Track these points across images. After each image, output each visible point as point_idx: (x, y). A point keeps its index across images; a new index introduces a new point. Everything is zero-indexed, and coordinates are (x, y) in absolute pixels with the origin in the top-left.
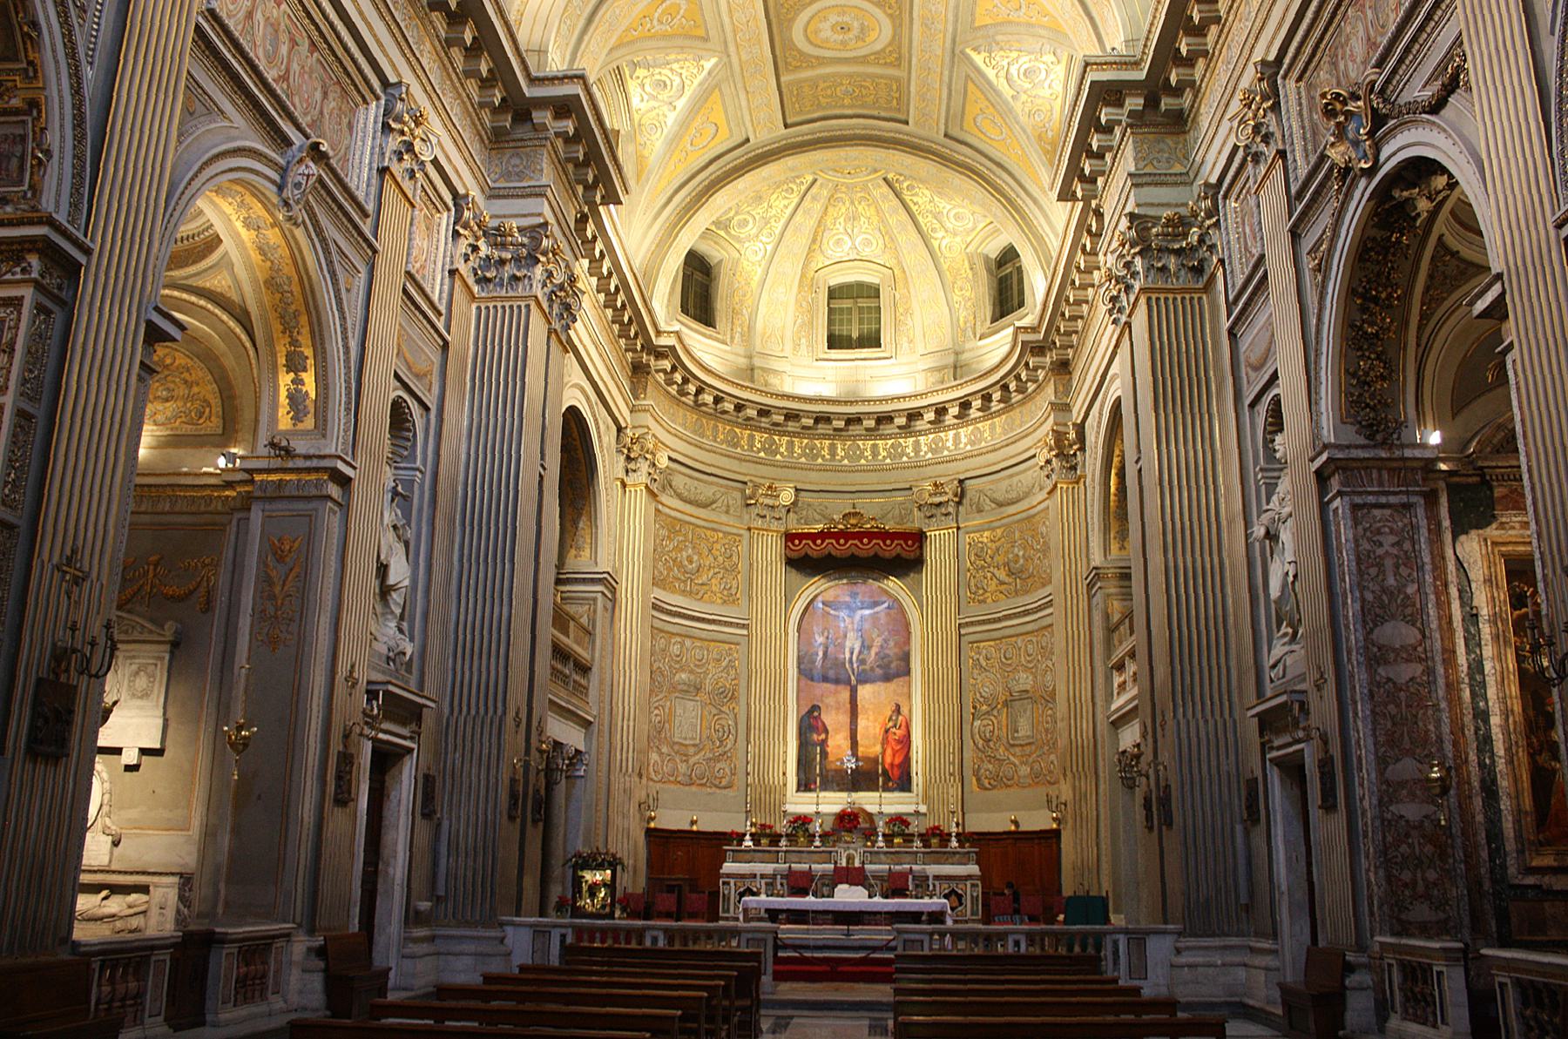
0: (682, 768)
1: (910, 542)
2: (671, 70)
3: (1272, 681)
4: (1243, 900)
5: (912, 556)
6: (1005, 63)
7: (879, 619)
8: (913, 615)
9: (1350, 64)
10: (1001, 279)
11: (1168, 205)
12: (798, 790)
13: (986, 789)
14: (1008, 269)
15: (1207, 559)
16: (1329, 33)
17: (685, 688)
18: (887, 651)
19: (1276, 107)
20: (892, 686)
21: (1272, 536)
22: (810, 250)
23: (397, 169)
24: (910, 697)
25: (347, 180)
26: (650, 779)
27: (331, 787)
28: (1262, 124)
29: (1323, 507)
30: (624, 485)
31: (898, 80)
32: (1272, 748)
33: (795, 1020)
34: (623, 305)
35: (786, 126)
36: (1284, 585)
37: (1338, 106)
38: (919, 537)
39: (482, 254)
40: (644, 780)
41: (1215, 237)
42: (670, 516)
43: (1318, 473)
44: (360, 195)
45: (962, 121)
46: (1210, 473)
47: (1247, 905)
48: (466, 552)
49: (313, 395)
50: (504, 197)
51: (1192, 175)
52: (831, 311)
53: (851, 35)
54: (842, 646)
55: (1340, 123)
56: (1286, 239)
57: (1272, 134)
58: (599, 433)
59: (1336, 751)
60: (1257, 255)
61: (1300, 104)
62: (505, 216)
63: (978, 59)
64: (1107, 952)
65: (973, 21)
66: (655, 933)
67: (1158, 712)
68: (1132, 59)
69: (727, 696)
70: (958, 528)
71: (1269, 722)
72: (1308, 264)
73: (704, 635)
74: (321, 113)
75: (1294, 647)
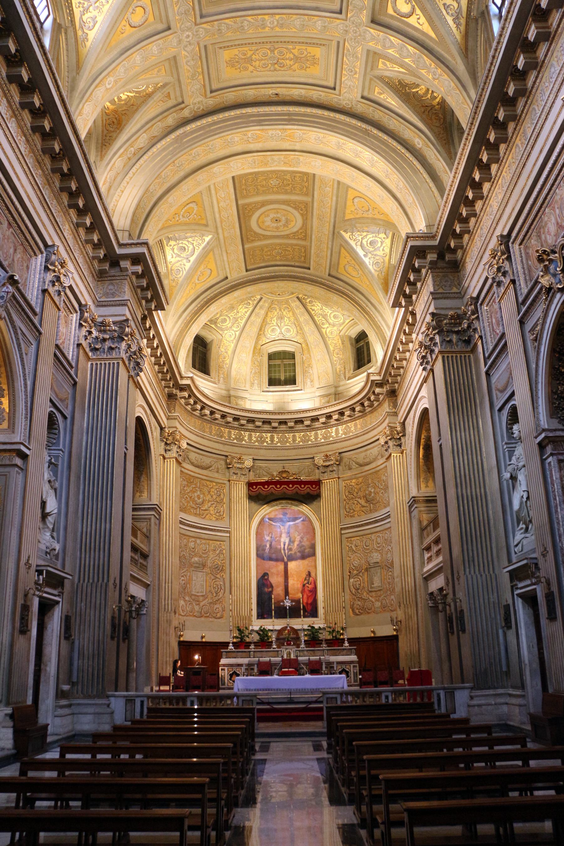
0: (197, 608)
2: (188, 241)
3: (516, 553)
4: (504, 669)
5: (315, 493)
6: (360, 238)
7: (298, 527)
8: (317, 525)
9: (548, 237)
11: (451, 309)
12: (258, 618)
13: (357, 615)
14: (361, 343)
15: (478, 490)
16: (536, 221)
17: (197, 565)
19: (509, 258)
20: (306, 562)
21: (513, 478)
22: (259, 335)
23: (51, 290)
25: (26, 295)
26: (180, 615)
27: (18, 625)
28: (501, 267)
29: (543, 461)
30: (164, 458)
31: (305, 247)
32: (517, 588)
33: (272, 744)
34: (164, 363)
35: (247, 271)
36: (521, 503)
37: (545, 257)
38: (318, 483)
39: (93, 336)
40: (177, 615)
41: (476, 324)
43: (540, 444)
44: (33, 303)
45: (338, 268)
46: (478, 446)
47: (506, 672)
48: (86, 494)
49: (7, 410)
50: (105, 306)
51: (463, 293)
52: (270, 366)
53: (281, 224)
54: (279, 542)
55: (545, 266)
56: (517, 325)
57: (507, 272)
58: (151, 430)
59: (555, 588)
60: (500, 334)
61: (521, 257)
62: (105, 316)
63: (347, 236)
64: (435, 700)
65: (344, 216)
66: (192, 699)
67: (455, 572)
68: (431, 235)
69: (218, 569)
71: (516, 575)
72: (530, 337)
74: (13, 260)
75: (527, 535)
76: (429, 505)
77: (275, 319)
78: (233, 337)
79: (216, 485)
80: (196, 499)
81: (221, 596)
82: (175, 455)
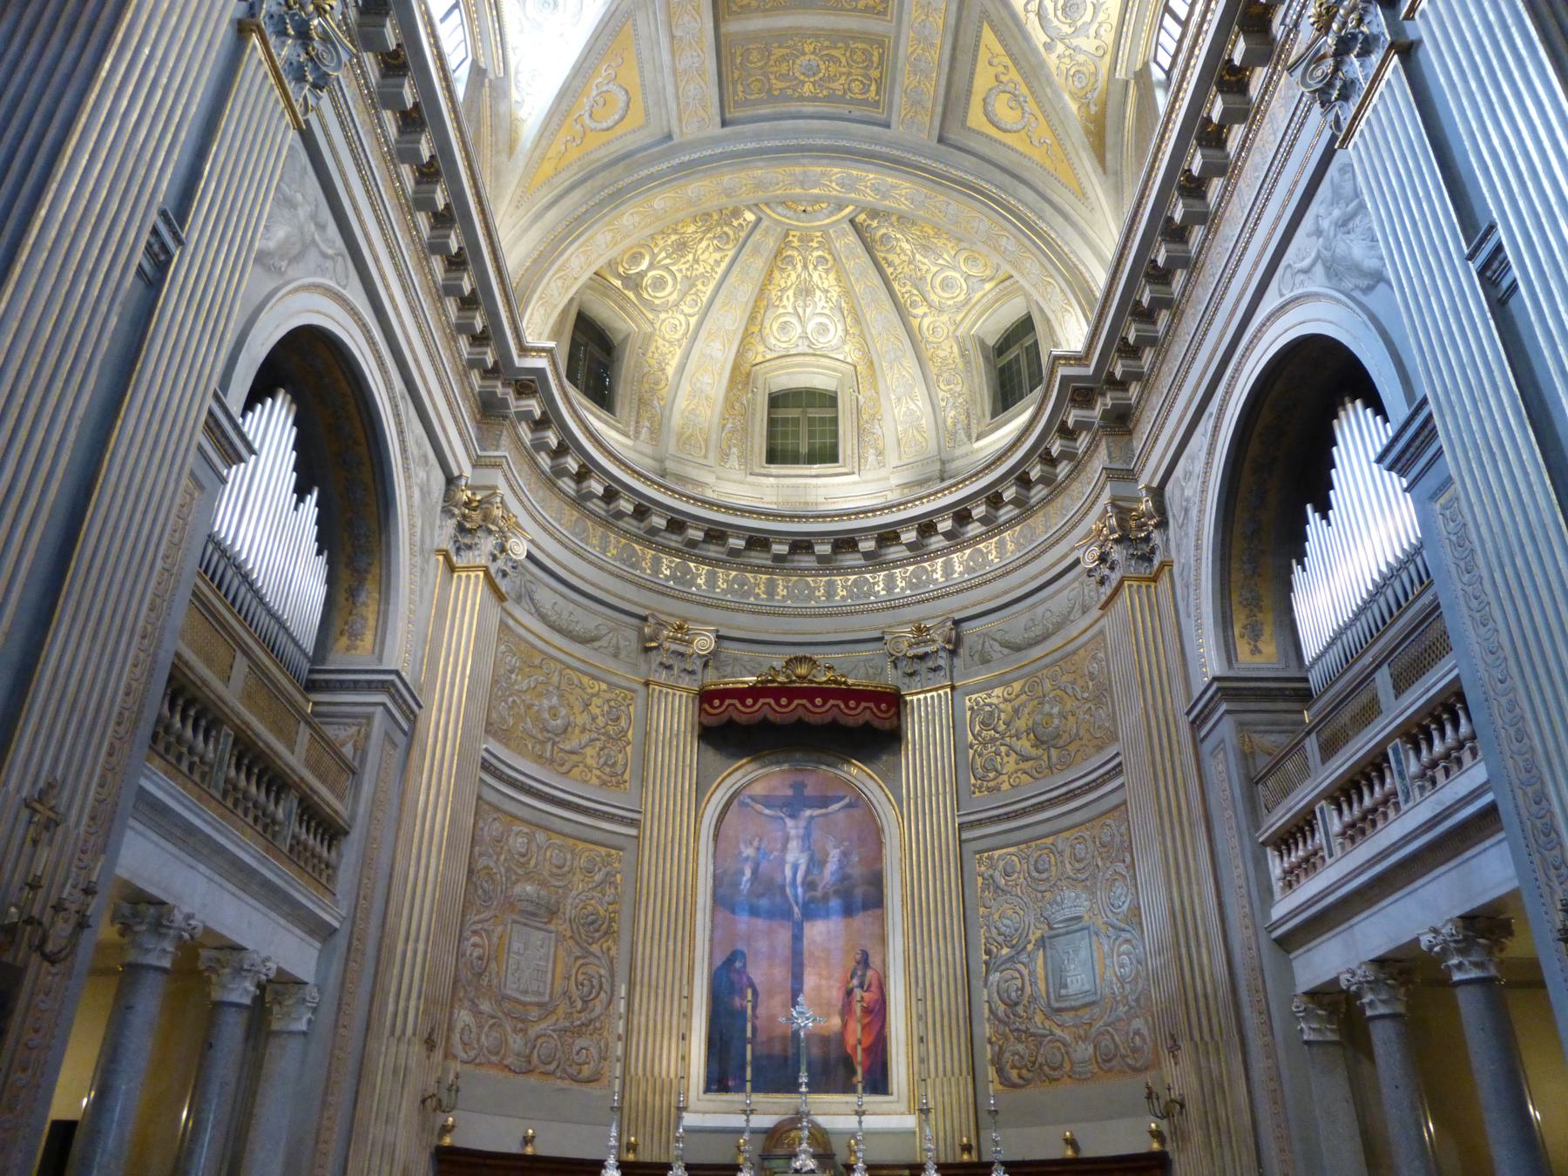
0: (516, 1042)
1: (883, 706)
5: (887, 725)
8: (888, 815)
10: (1002, 371)
12: (707, 1090)
13: (1014, 1086)
18: (849, 870)
22: (747, 334)
24: (883, 940)
30: (452, 568)
35: (724, 123)
38: (893, 701)
40: (438, 1055)
42: (527, 642)
52: (772, 422)
54: (782, 862)
69: (597, 928)
70: (953, 688)
73: (568, 828)
77: (790, 293)
78: (681, 331)
79: (610, 690)
80: (547, 716)
81: (598, 1010)
82: (483, 561)
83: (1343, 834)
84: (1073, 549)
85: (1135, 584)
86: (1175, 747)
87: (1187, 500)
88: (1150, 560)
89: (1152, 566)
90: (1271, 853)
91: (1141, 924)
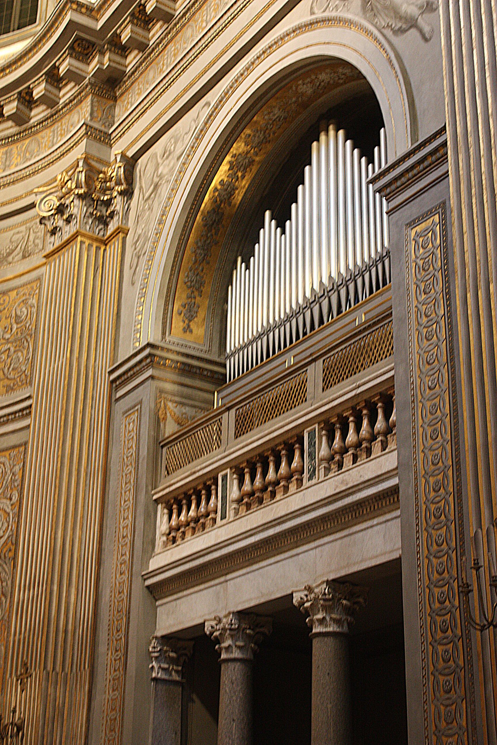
76: (188, 381)
83: (239, 501)
84: (31, 192)
85: (87, 242)
86: (89, 401)
87: (161, 177)
88: (106, 224)
89: (106, 230)
90: (161, 511)
91: (15, 558)
